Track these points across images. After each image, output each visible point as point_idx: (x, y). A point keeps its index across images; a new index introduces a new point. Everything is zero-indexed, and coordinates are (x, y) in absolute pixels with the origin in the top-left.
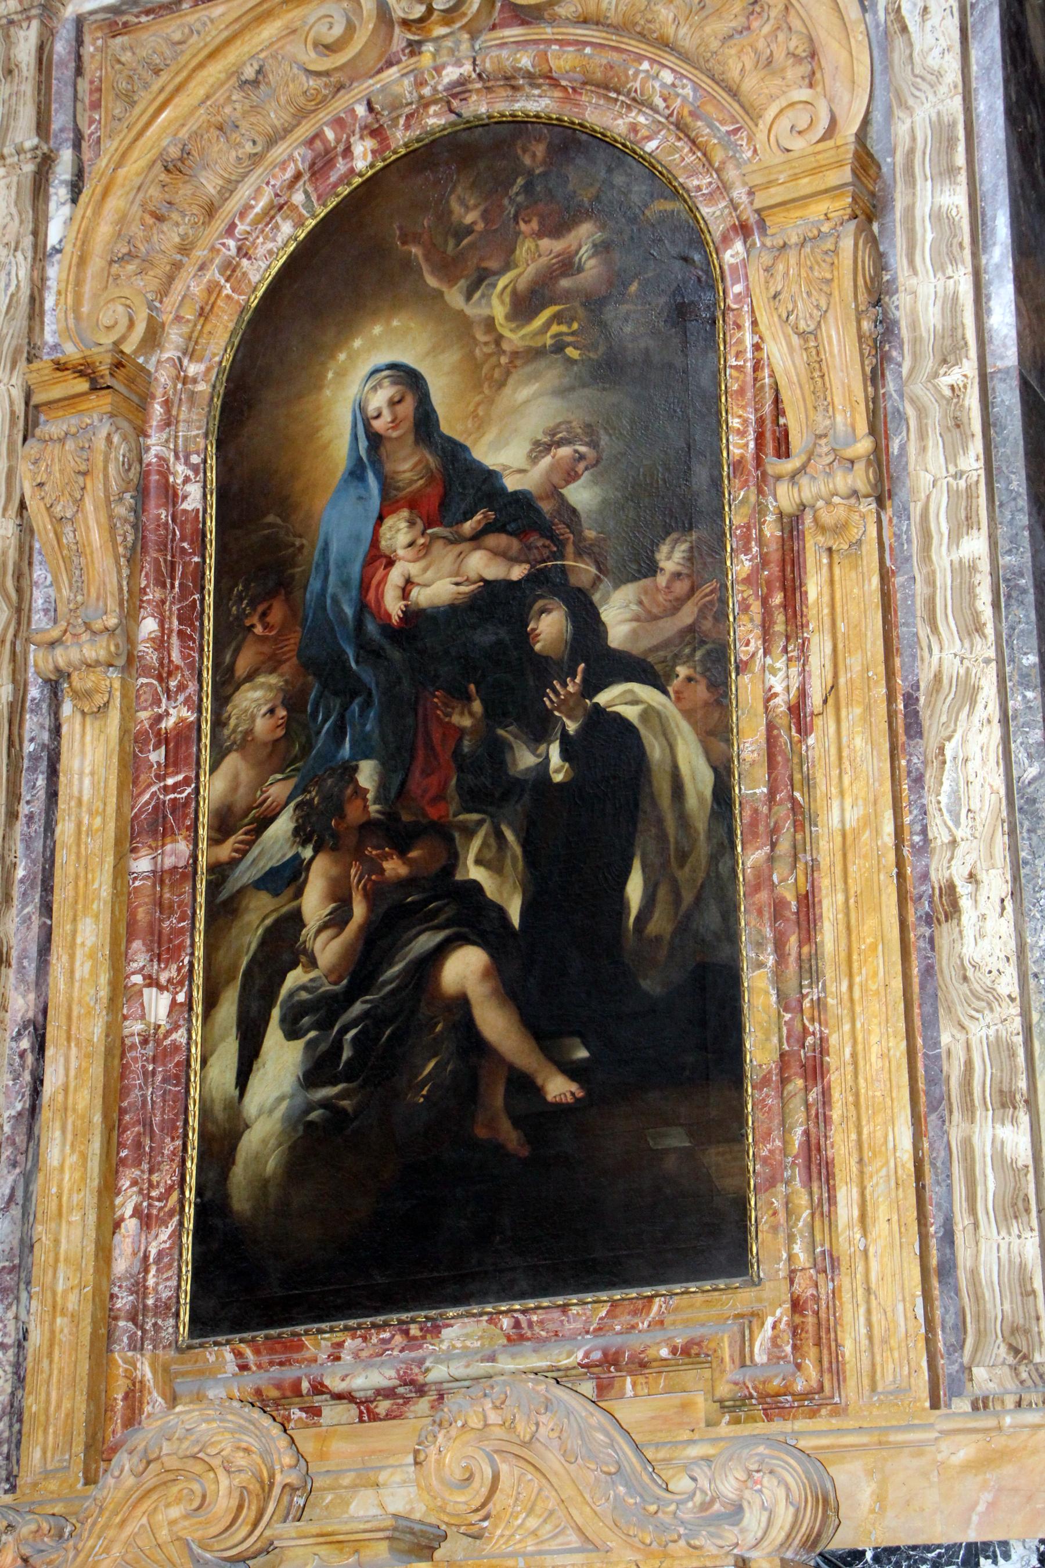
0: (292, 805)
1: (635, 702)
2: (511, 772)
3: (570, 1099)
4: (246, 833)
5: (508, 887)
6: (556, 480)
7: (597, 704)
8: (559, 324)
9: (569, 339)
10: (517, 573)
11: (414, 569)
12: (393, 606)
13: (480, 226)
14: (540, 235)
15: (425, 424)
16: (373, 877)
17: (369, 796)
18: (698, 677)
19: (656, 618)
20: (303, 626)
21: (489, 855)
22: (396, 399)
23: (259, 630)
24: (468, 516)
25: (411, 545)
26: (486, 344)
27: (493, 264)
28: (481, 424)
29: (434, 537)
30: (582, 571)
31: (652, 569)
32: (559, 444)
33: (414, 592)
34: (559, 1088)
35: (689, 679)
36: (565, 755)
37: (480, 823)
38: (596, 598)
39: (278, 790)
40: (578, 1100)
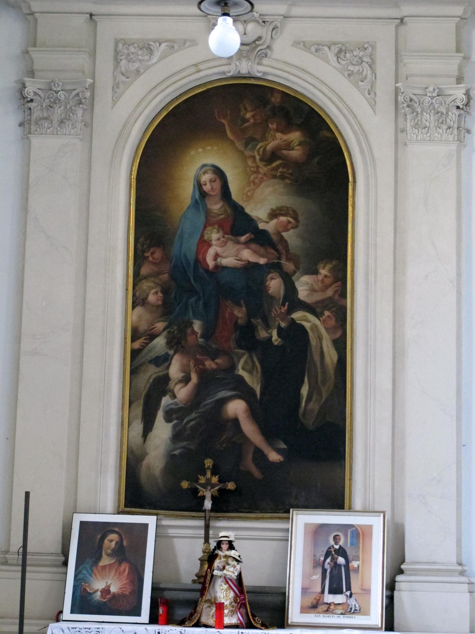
0: (165, 333)
1: (308, 321)
2: (258, 338)
3: (278, 461)
4: (145, 339)
5: (255, 381)
6: (280, 230)
7: (293, 319)
8: (283, 168)
9: (287, 175)
10: (262, 261)
11: (219, 250)
12: (211, 263)
13: (252, 121)
14: (277, 130)
15: (225, 193)
16: (200, 367)
17: (199, 335)
18: (332, 316)
19: (316, 291)
20: (171, 262)
21: (248, 367)
22: (213, 180)
23: (151, 259)
24: (242, 235)
25: (218, 239)
26: (253, 167)
27: (258, 137)
28: (249, 198)
29: (228, 239)
30: (289, 266)
31: (316, 272)
32: (282, 215)
33: (219, 259)
34: (274, 457)
35: (329, 316)
36: (279, 335)
37: (244, 354)
38: (294, 278)
39: (160, 326)
40: (281, 461)
